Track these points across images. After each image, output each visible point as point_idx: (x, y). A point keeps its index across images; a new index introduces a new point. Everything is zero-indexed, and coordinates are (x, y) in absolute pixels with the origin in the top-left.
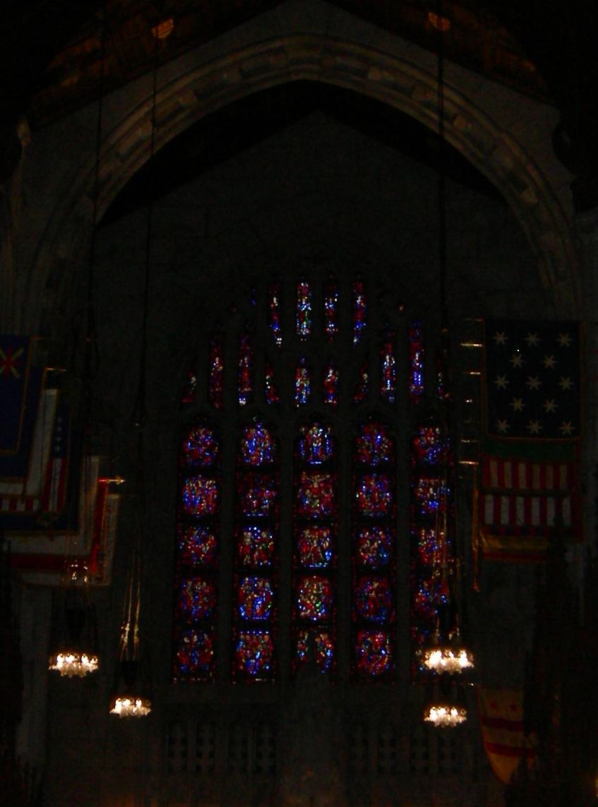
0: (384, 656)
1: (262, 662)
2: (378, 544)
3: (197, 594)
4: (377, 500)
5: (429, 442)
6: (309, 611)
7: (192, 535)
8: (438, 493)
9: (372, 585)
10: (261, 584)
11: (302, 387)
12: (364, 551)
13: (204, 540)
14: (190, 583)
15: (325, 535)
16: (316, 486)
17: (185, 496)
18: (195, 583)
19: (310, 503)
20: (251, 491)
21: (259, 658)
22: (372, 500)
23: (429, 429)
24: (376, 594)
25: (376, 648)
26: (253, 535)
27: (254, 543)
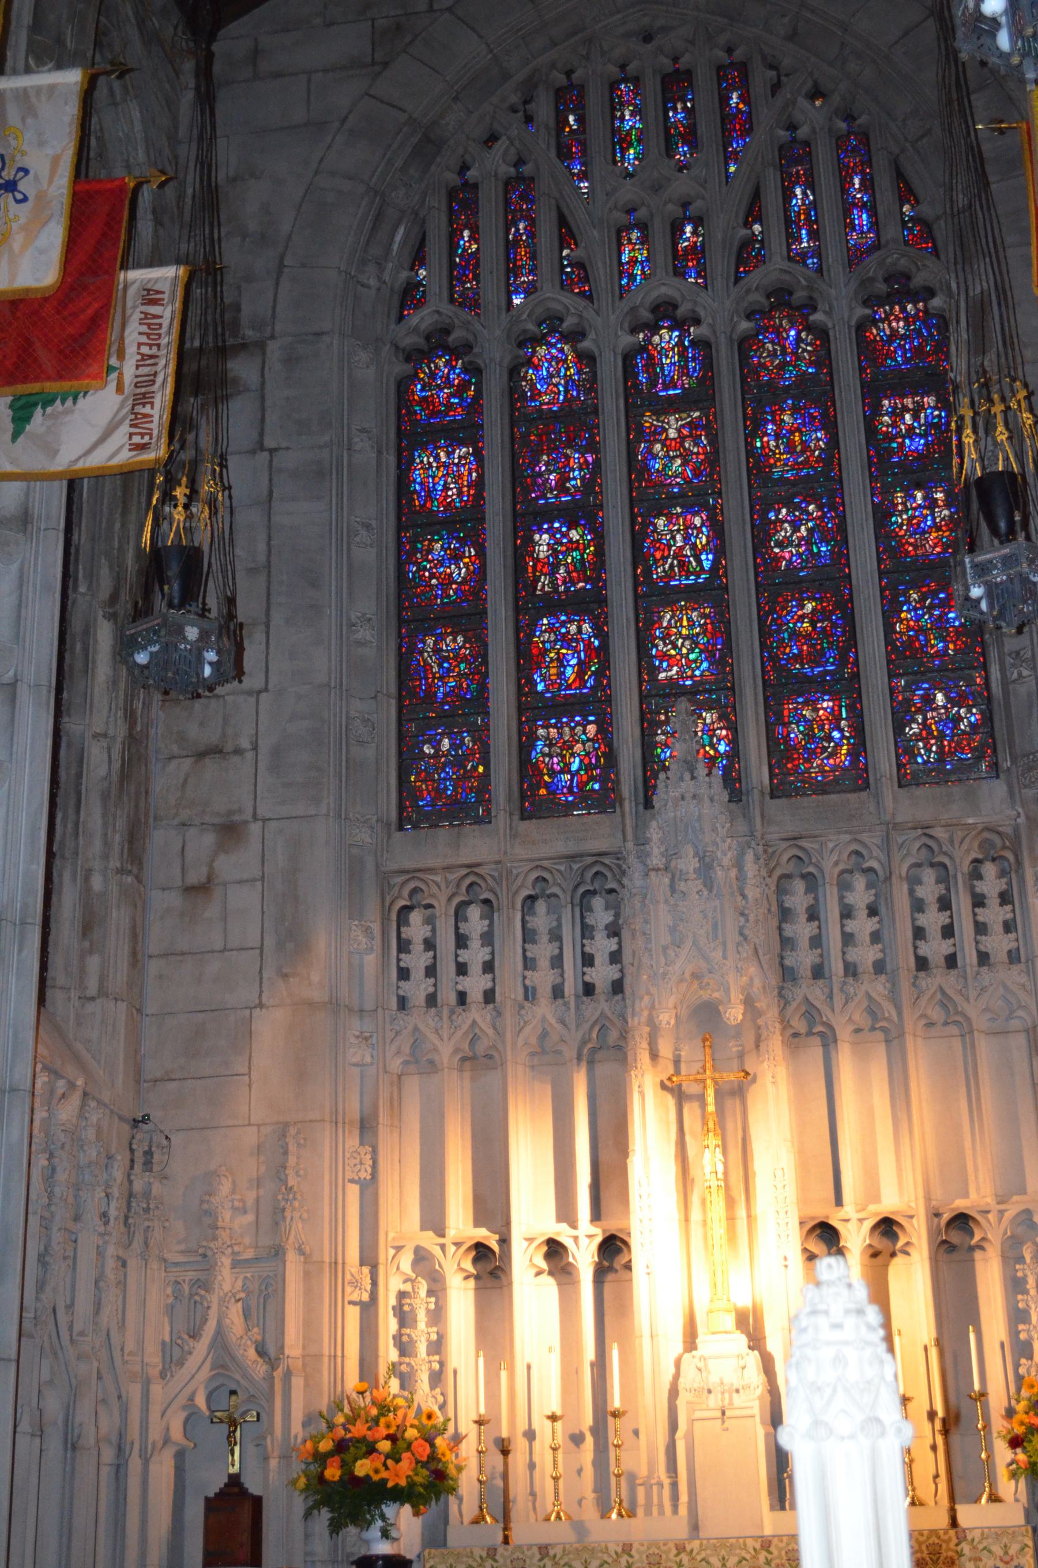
0: (839, 745)
1: (585, 779)
2: (807, 530)
3: (446, 659)
4: (799, 448)
5: (894, 332)
6: (675, 669)
7: (430, 551)
8: (922, 421)
9: (802, 607)
10: (573, 628)
11: (633, 261)
12: (779, 544)
13: (456, 557)
14: (430, 641)
15: (697, 521)
16: (672, 434)
17: (414, 481)
18: (440, 638)
19: (665, 466)
20: (545, 457)
21: (580, 769)
22: (790, 448)
23: (892, 308)
24: (813, 624)
25: (821, 728)
26: (552, 536)
27: (555, 553)
